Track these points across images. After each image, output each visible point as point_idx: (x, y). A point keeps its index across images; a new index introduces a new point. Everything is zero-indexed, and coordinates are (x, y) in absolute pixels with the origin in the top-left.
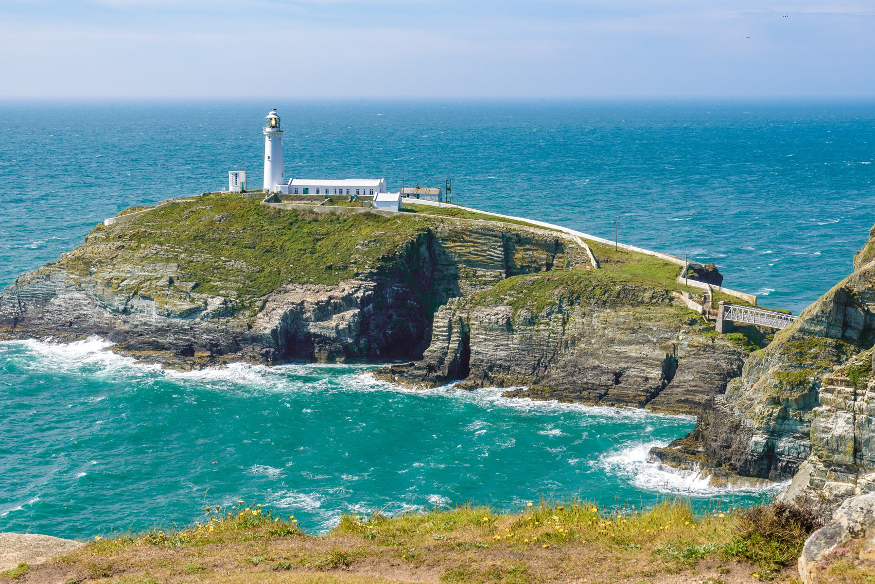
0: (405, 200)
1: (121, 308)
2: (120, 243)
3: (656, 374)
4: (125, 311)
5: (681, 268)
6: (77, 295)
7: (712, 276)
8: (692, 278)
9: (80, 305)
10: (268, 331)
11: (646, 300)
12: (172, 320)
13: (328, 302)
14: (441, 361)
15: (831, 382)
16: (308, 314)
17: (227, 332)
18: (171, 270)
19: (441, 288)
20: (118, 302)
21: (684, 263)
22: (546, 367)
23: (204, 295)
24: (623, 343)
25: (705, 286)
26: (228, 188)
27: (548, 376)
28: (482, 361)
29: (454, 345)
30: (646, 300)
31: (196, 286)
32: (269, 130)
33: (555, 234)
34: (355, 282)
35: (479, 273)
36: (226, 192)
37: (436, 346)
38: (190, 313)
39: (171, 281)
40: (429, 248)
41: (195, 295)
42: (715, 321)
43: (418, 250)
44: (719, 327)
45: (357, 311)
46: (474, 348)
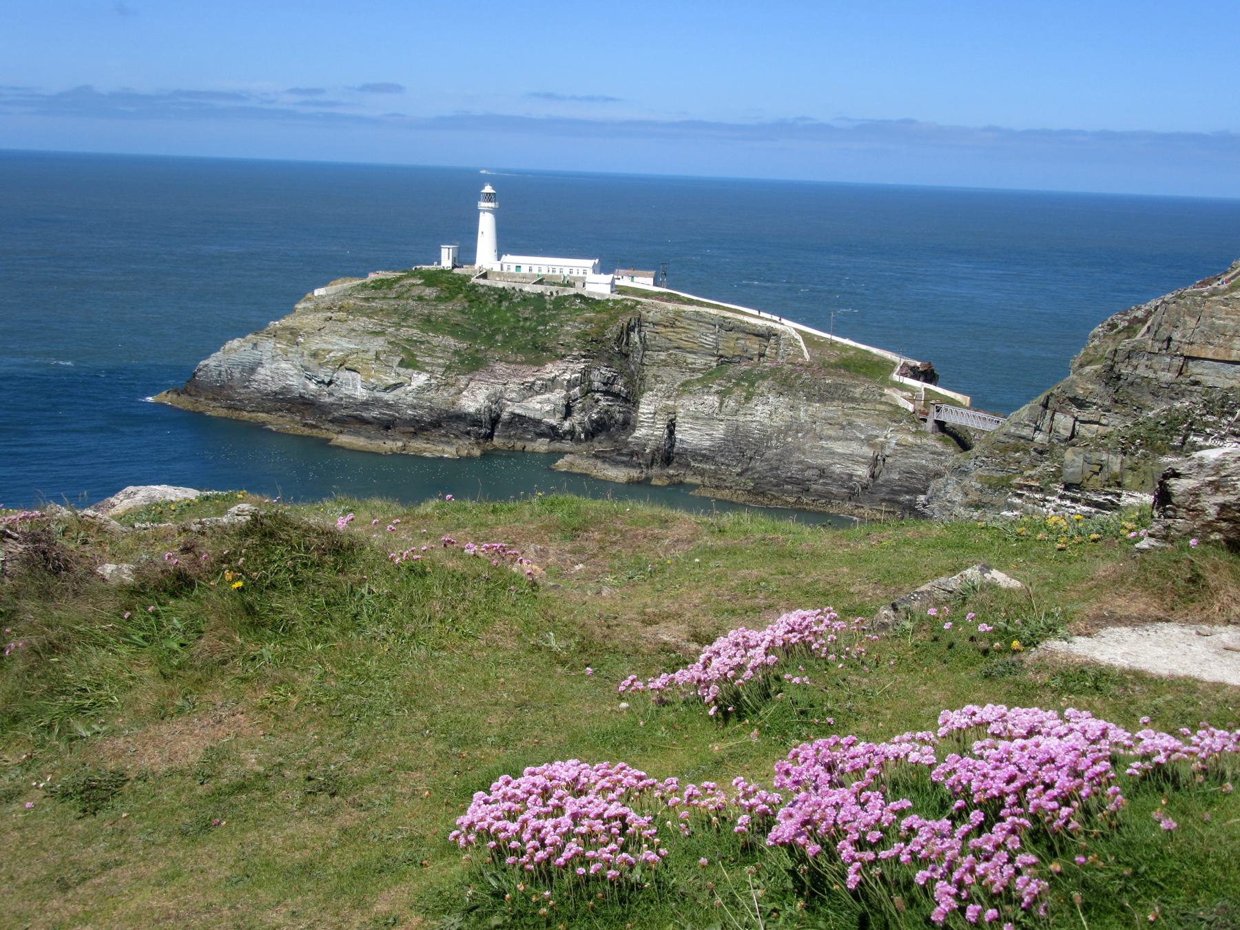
0: (617, 283)
1: (327, 380)
2: (329, 314)
3: (863, 471)
4: (330, 383)
5: (895, 364)
6: (284, 365)
7: (928, 376)
8: (905, 375)
9: (285, 376)
12: (378, 395)
13: (533, 383)
14: (645, 445)
15: (1021, 487)
16: (514, 395)
17: (431, 409)
18: (379, 344)
19: (650, 374)
20: (324, 375)
22: (751, 458)
23: (410, 370)
24: (830, 438)
25: (918, 384)
26: (439, 263)
27: (752, 468)
28: (686, 450)
30: (857, 396)
31: (402, 361)
32: (483, 205)
33: (769, 324)
34: (562, 366)
35: (689, 361)
36: (440, 267)
40: (640, 331)
41: (402, 370)
42: (925, 420)
43: (628, 335)
44: (929, 425)
46: (679, 436)
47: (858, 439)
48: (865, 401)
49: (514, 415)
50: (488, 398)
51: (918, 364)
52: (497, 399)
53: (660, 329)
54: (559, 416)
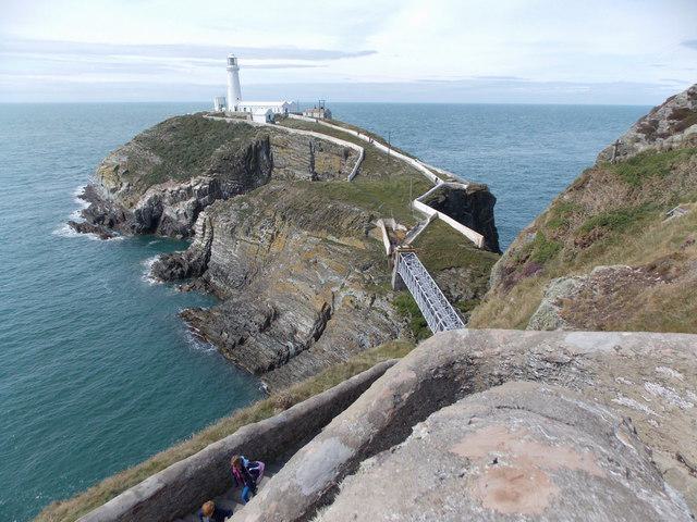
10: (134, 211)
11: (344, 226)
13: (178, 192)
16: (166, 200)
25: (431, 212)
29: (203, 245)
30: (344, 226)
37: (197, 241)
38: (113, 191)
39: (117, 168)
45: (193, 200)
47: (318, 282)
48: (348, 235)
50: (150, 202)
51: (465, 187)
52: (157, 203)
53: (279, 150)
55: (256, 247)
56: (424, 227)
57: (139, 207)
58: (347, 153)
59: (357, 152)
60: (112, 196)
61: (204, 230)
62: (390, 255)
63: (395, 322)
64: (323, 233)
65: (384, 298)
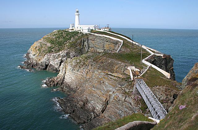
21: (152, 54)
25: (149, 64)
30: (115, 69)
37: (60, 73)
38: (34, 55)
43: (84, 43)
45: (60, 58)
48: (116, 72)
49: (51, 64)
51: (162, 55)
53: (92, 41)
54: (58, 65)
55: (81, 76)
56: (146, 70)
57: (42, 61)
58: (116, 43)
59: (120, 42)
60: (34, 57)
61: (63, 69)
62: (133, 81)
63: (134, 107)
64: (107, 72)
65: (130, 97)
